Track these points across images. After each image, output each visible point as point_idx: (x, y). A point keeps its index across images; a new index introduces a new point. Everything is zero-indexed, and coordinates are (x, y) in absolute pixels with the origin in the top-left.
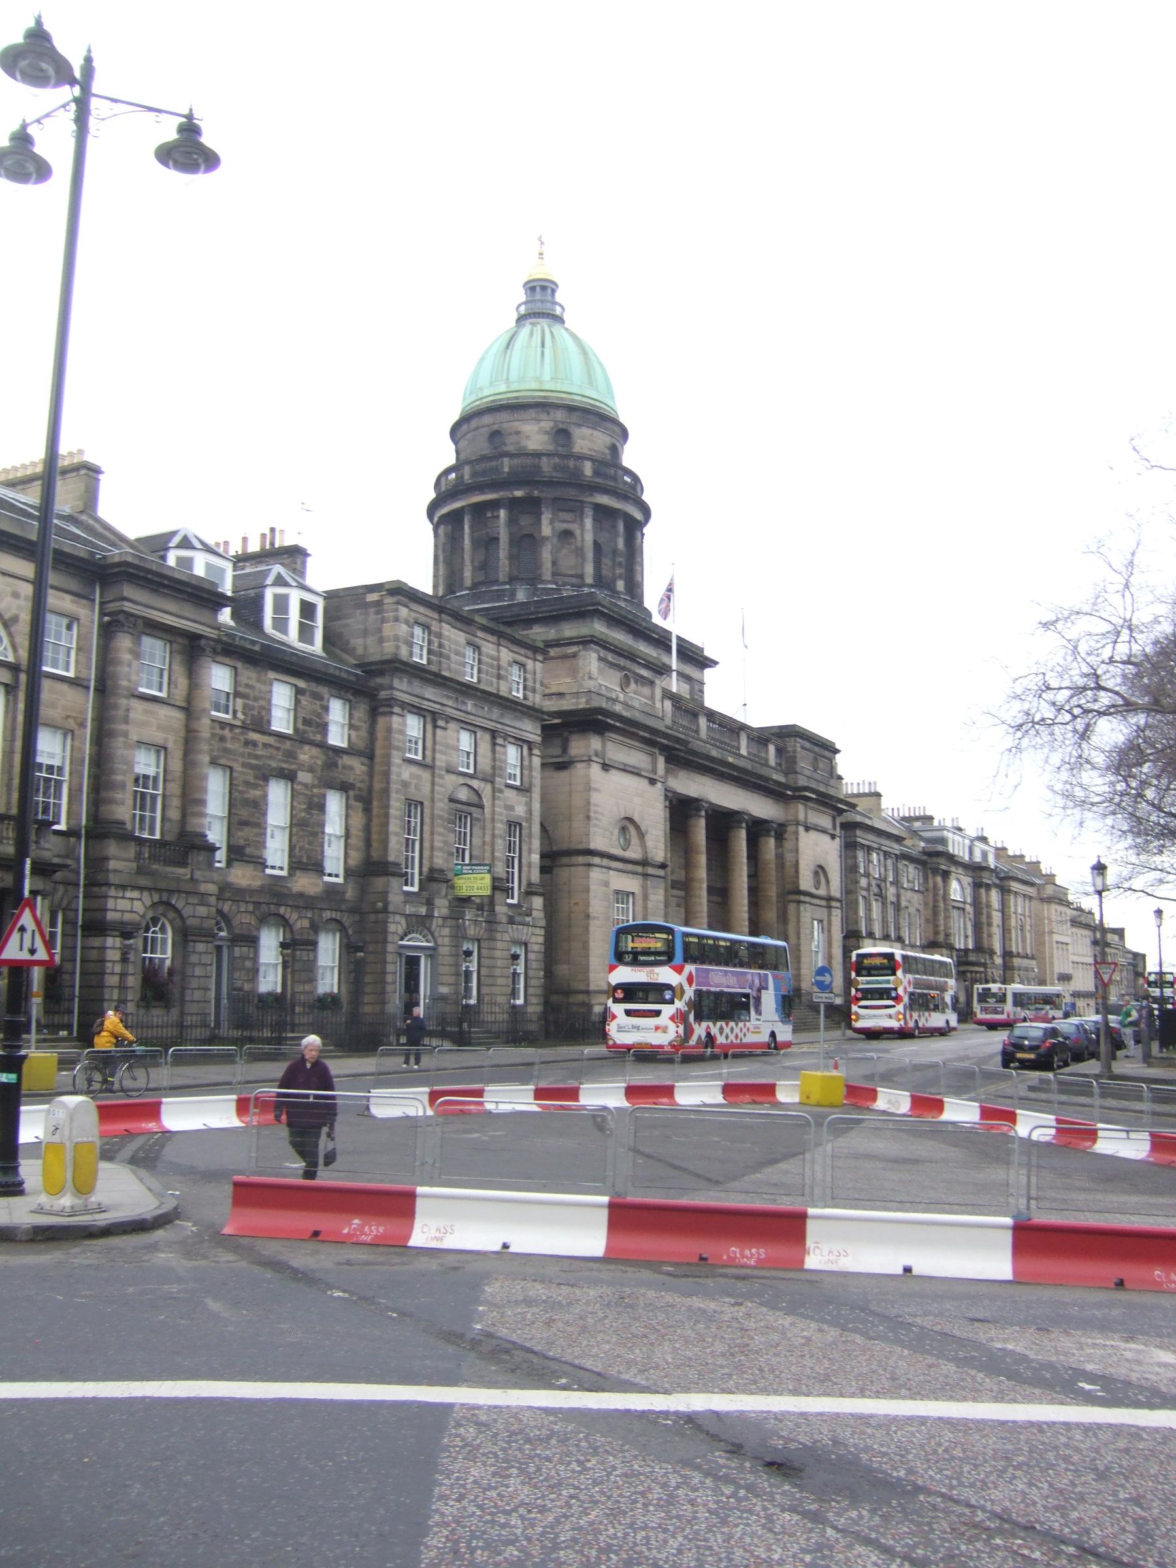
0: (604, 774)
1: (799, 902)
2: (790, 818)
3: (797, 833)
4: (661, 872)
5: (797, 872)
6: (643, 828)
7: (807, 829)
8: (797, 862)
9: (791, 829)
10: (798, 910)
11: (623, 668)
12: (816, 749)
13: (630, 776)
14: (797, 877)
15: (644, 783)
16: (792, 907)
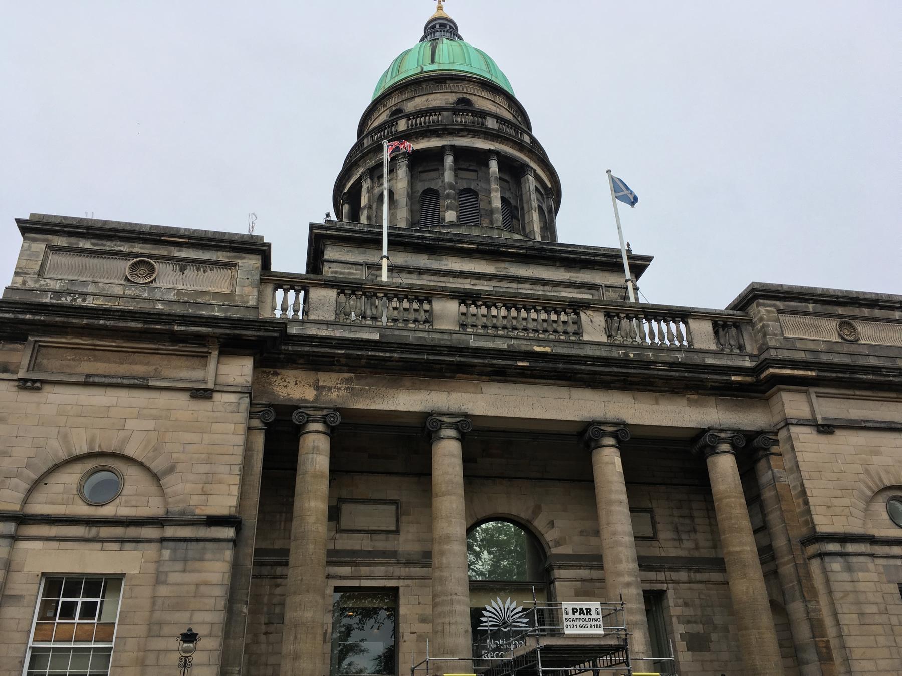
0: (27, 397)
1: (822, 555)
2: (777, 418)
3: (790, 438)
4: (229, 532)
5: (806, 503)
6: (157, 465)
7: (826, 428)
8: (802, 485)
9: (782, 435)
10: (825, 572)
11: (129, 255)
12: (840, 311)
13: (123, 393)
14: (809, 512)
15: (182, 399)
16: (815, 565)
